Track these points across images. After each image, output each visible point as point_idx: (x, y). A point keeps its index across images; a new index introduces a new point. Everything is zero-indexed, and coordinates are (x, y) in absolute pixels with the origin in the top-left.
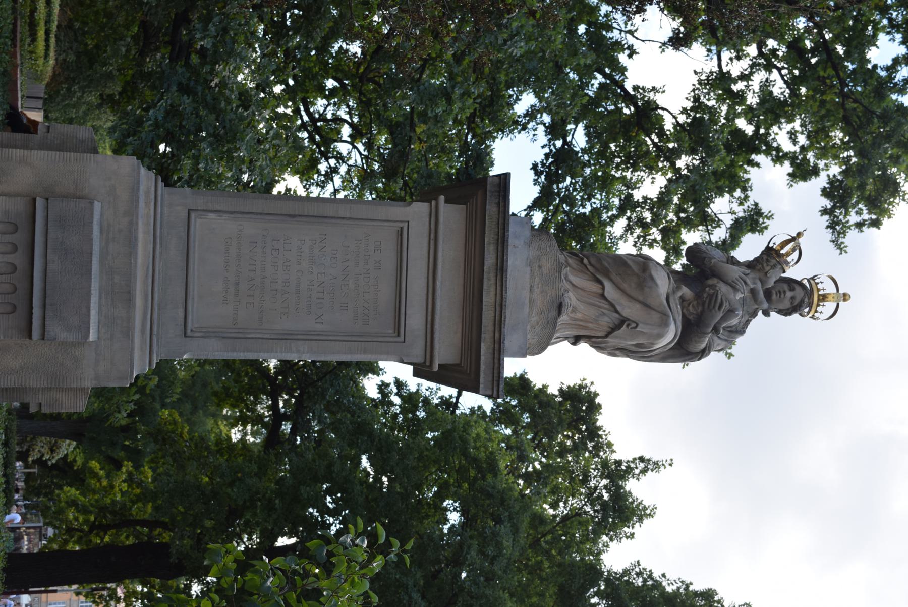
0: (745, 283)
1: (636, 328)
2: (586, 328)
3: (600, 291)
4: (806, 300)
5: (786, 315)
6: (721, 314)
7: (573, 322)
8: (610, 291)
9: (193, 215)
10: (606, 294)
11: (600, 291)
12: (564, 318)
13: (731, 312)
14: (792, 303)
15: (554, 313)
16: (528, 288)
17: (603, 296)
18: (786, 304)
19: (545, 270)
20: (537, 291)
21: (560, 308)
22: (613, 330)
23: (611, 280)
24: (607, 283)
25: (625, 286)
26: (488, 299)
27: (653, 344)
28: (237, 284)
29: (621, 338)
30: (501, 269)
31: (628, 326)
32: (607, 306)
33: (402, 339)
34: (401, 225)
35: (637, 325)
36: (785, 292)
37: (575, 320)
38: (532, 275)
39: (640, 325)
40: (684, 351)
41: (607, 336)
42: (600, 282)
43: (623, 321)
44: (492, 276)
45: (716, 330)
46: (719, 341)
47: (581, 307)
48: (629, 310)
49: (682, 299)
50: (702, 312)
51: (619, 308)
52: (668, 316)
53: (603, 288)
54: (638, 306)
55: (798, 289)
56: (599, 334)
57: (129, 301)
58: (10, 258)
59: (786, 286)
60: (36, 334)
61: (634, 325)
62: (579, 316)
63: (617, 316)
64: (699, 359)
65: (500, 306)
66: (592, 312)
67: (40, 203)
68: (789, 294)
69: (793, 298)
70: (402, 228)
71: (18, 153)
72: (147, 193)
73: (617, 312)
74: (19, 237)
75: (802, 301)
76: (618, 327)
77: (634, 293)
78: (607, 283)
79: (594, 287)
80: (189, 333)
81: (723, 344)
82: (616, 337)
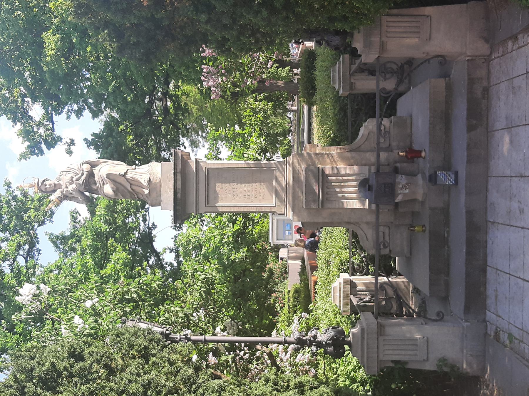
3: (132, 186)
11: (132, 186)
17: (131, 184)
19: (155, 192)
24: (130, 189)
25: (123, 188)
26: (179, 183)
41: (128, 170)
42: (132, 189)
45: (83, 174)
49: (95, 184)
67: (321, 207)
70: (208, 204)
71: (326, 221)
77: (119, 186)
78: (130, 189)
79: (134, 187)
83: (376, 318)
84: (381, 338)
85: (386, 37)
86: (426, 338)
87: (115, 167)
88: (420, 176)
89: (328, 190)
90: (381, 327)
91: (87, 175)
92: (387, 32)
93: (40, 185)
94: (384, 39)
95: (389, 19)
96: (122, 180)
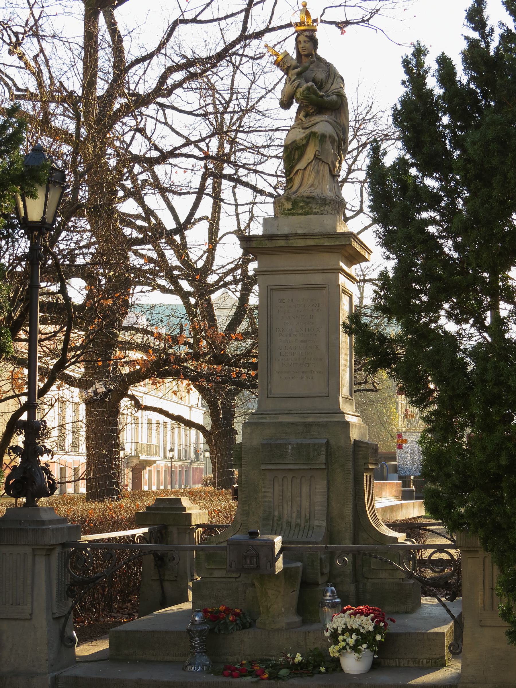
2: (323, 176)
3: (302, 171)
5: (317, 43)
9: (270, 396)
11: (302, 171)
17: (305, 169)
24: (297, 168)
27: (330, 137)
28: (303, 372)
30: (287, 237)
32: (310, 166)
33: (327, 286)
42: (297, 171)
45: (322, 97)
51: (310, 161)
56: (327, 167)
59: (300, 46)
64: (345, 97)
65: (305, 236)
69: (305, 42)
73: (312, 162)
76: (320, 160)
79: (300, 173)
80: (327, 395)
90: (49, 550)
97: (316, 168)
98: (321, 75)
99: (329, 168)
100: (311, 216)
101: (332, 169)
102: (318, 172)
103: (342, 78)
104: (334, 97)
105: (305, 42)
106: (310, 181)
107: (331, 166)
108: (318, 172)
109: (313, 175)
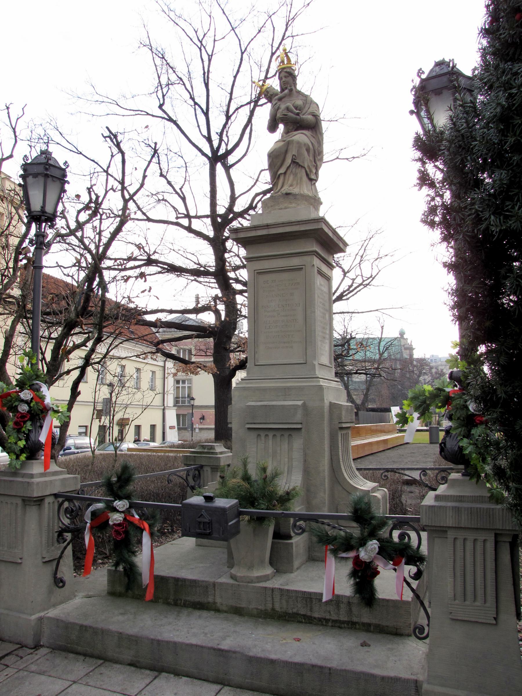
0: (276, 104)
1: (295, 155)
2: (301, 178)
4: (285, 70)
6: (290, 114)
7: (299, 186)
8: (282, 171)
10: (283, 172)
12: (296, 190)
13: (288, 109)
14: (288, 77)
15: (291, 197)
16: (280, 211)
17: (285, 173)
18: (290, 79)
20: (282, 206)
21: (287, 194)
22: (300, 165)
23: (278, 171)
25: (279, 164)
27: (305, 144)
28: (284, 342)
29: (307, 160)
30: (267, 226)
31: (295, 159)
34: (256, 273)
35: (293, 155)
36: (284, 82)
37: (297, 184)
38: (275, 209)
39: (294, 153)
40: (313, 126)
43: (294, 162)
44: (270, 230)
45: (298, 114)
46: (311, 108)
47: (290, 182)
48: (288, 161)
50: (291, 123)
51: (288, 165)
52: (289, 141)
53: (281, 174)
54: (287, 156)
55: (281, 76)
56: (304, 171)
57: (289, 388)
58: (271, 437)
60: (299, 426)
61: (294, 157)
62: (295, 183)
63: (291, 165)
66: (291, 177)
68: (284, 79)
69: (285, 77)
70: (257, 273)
72: (251, 383)
73: (290, 166)
74: (263, 434)
75: (286, 72)
76: (297, 164)
81: (313, 106)
82: (303, 162)
83: (56, 496)
84: (19, 501)
85: (455, 539)
86: (20, 561)
87: (308, 150)
88: (269, 571)
89: (271, 437)
91: (296, 119)
92: (465, 540)
93: (285, 70)
94: (451, 535)
95: (490, 546)
96: (288, 161)
97: (294, 170)
98: (299, 102)
99: (306, 172)
100: (288, 210)
101: (309, 172)
102: (295, 175)
103: (317, 105)
104: (310, 117)
105: (285, 77)
106: (290, 182)
107: (307, 170)
108: (295, 175)
109: (291, 177)
